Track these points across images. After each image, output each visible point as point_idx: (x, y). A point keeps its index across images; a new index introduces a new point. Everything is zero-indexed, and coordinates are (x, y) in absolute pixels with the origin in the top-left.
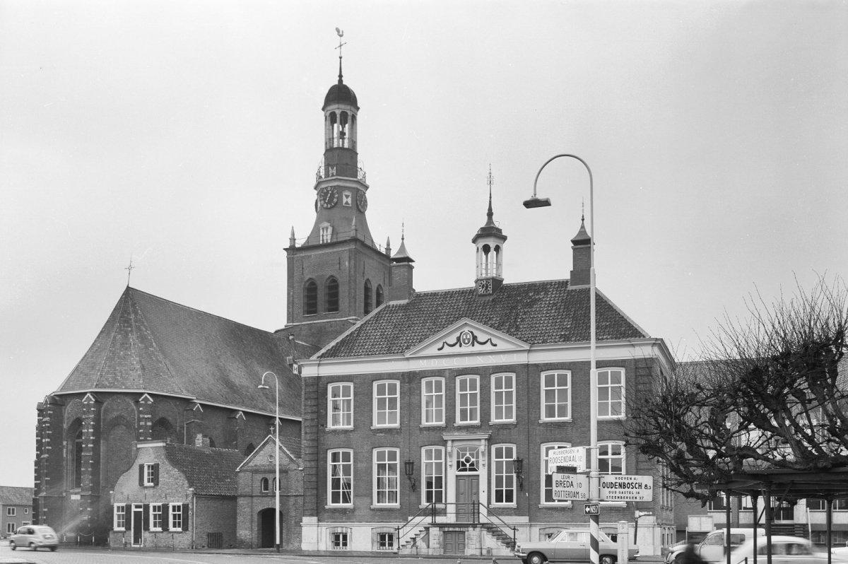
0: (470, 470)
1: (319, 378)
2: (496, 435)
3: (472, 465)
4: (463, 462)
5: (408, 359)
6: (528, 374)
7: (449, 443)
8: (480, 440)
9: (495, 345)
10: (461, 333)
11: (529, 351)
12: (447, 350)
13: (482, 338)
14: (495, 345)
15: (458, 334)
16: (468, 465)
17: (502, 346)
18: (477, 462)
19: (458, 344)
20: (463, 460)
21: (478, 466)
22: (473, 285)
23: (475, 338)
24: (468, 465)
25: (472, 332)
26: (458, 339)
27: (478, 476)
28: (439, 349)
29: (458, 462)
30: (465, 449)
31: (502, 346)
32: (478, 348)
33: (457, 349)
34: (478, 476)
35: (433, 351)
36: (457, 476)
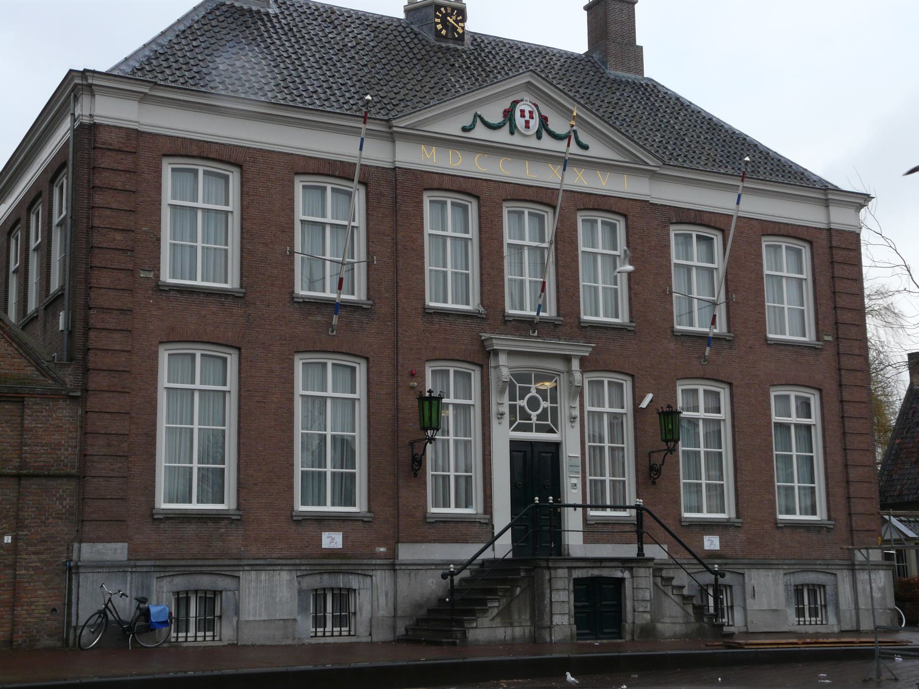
0: (540, 429)
1: (136, 135)
2: (606, 349)
3: (541, 417)
4: (522, 408)
5: (392, 137)
6: (647, 228)
7: (503, 359)
8: (567, 359)
9: (585, 147)
10: (515, 103)
11: (653, 175)
12: (480, 133)
13: (558, 125)
14: (585, 147)
15: (507, 105)
16: (534, 415)
17: (597, 150)
18: (554, 411)
19: (507, 128)
20: (524, 403)
21: (555, 421)
22: (401, 15)
23: (544, 120)
24: (534, 415)
25: (536, 106)
26: (509, 114)
27: (557, 446)
28: (464, 129)
29: (512, 408)
30: (524, 378)
31: (597, 150)
32: (547, 143)
33: (502, 136)
34: (557, 446)
35: (452, 127)
36: (515, 446)
